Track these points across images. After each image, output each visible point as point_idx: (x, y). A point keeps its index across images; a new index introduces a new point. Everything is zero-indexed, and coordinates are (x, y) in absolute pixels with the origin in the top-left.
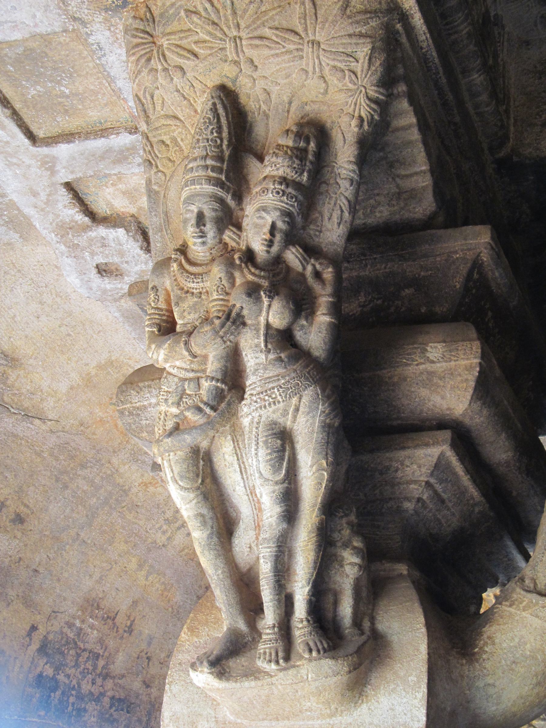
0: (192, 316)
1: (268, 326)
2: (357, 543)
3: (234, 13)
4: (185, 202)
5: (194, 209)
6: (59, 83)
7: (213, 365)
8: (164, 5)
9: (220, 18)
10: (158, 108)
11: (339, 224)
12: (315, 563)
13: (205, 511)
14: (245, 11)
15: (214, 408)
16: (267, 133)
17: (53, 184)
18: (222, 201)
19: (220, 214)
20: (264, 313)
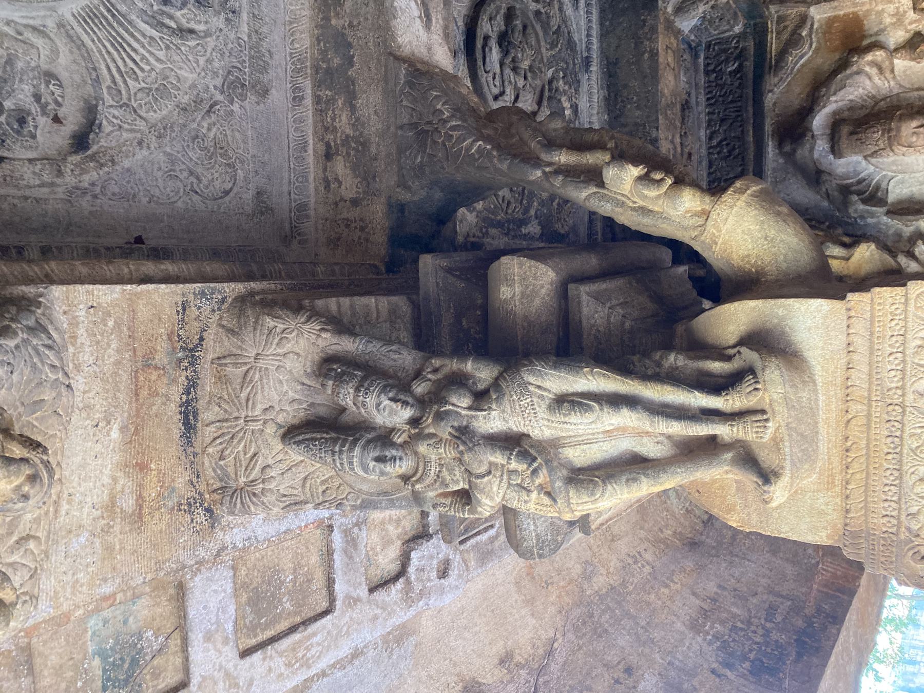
0: (457, 473)
1: (470, 408)
2: (657, 355)
3: (226, 420)
4: (366, 472)
5: (372, 464)
6: (282, 582)
7: (498, 458)
8: (213, 478)
9: (229, 432)
10: (296, 492)
11: (400, 354)
12: (674, 385)
13: (624, 478)
14: (226, 411)
15: (534, 459)
16: (324, 405)
17: (368, 602)
18: (369, 442)
19: (379, 444)
20: (459, 410)
